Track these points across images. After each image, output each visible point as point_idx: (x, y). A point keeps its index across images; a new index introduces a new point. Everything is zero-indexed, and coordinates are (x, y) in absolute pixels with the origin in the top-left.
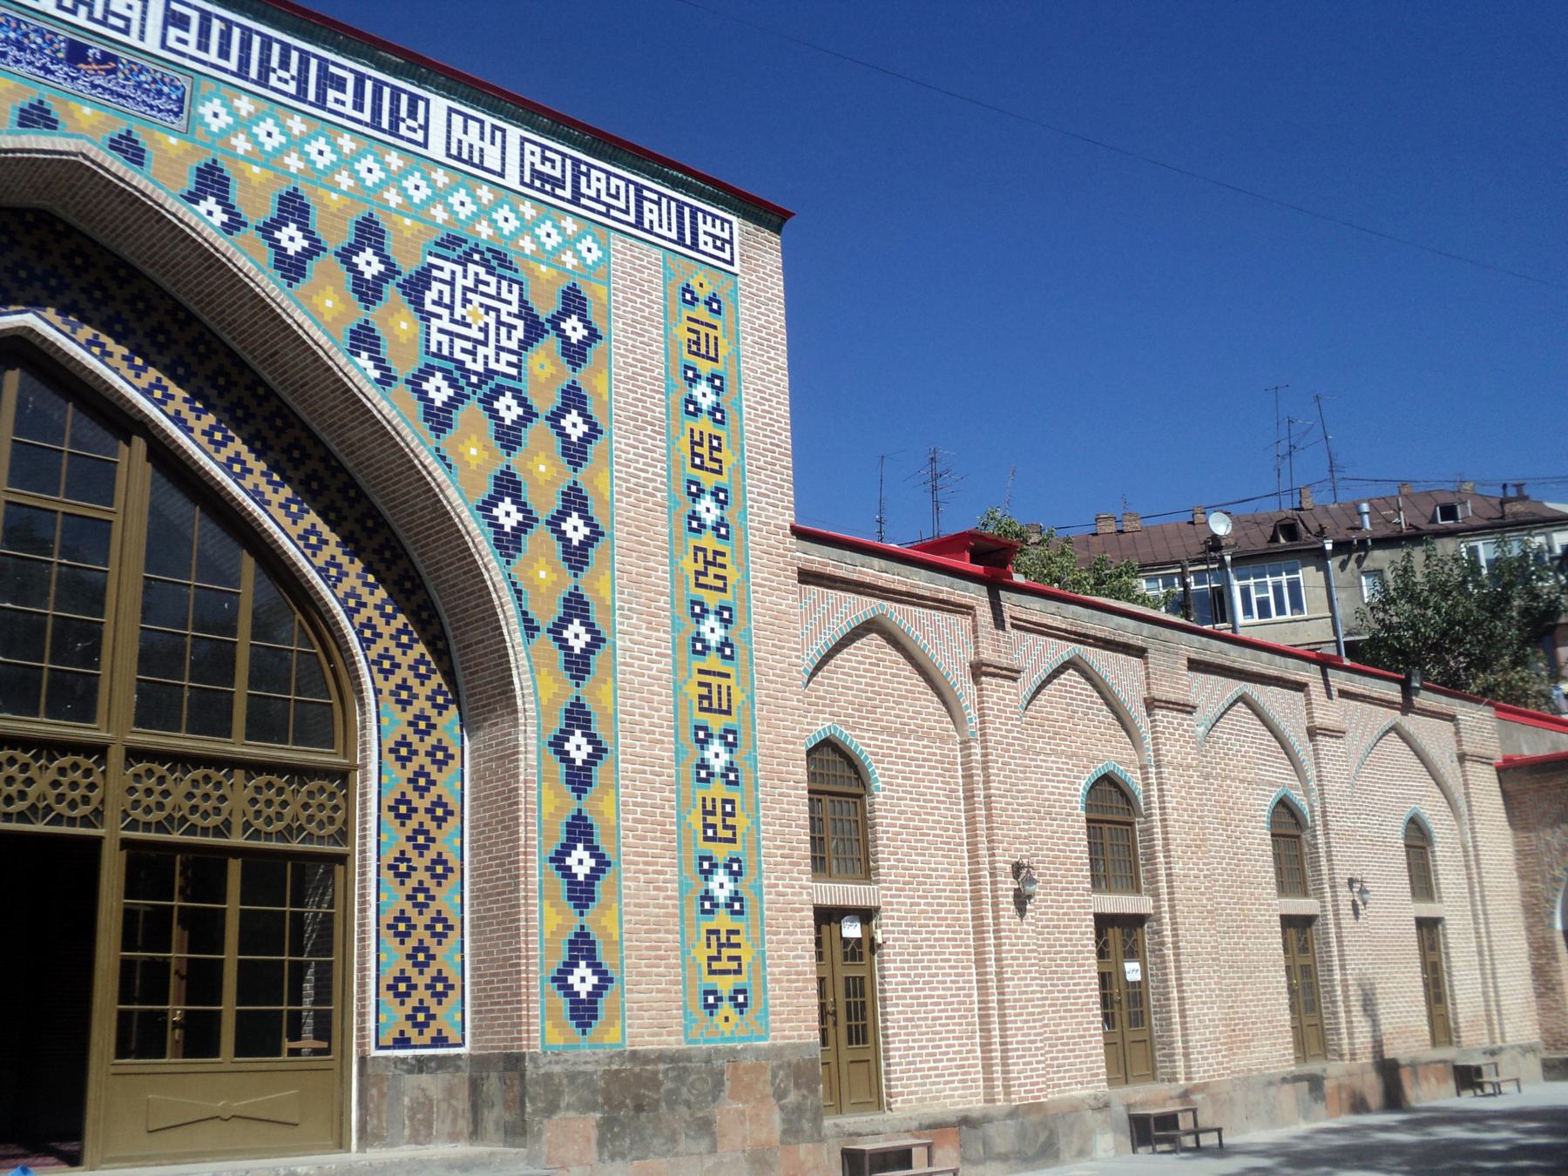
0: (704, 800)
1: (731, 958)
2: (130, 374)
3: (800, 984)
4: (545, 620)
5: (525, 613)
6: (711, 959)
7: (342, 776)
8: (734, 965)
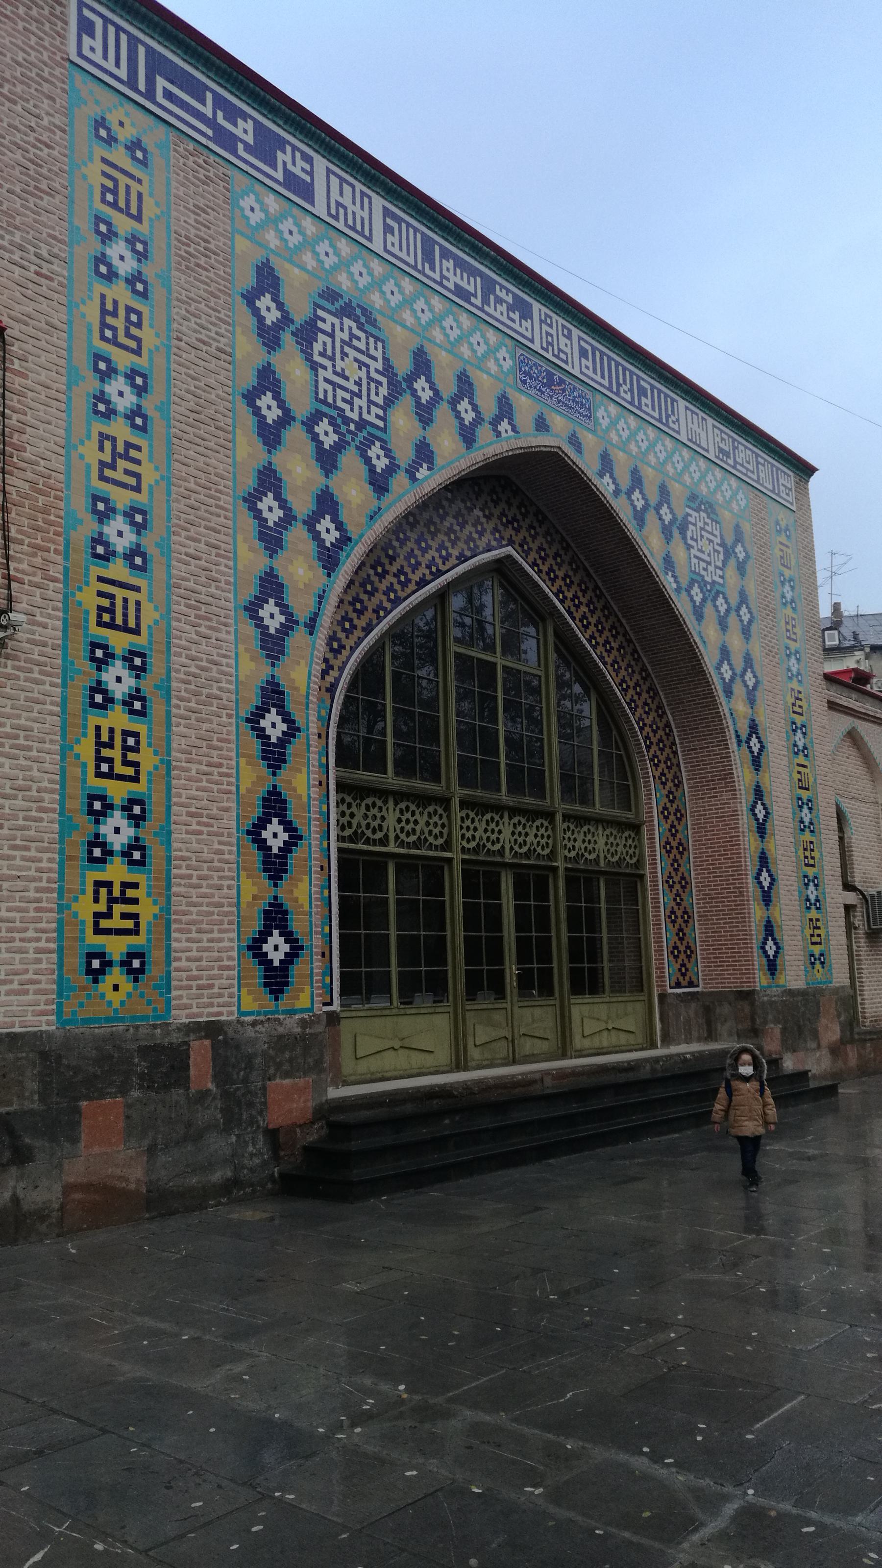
2: (549, 583)
7: (636, 828)
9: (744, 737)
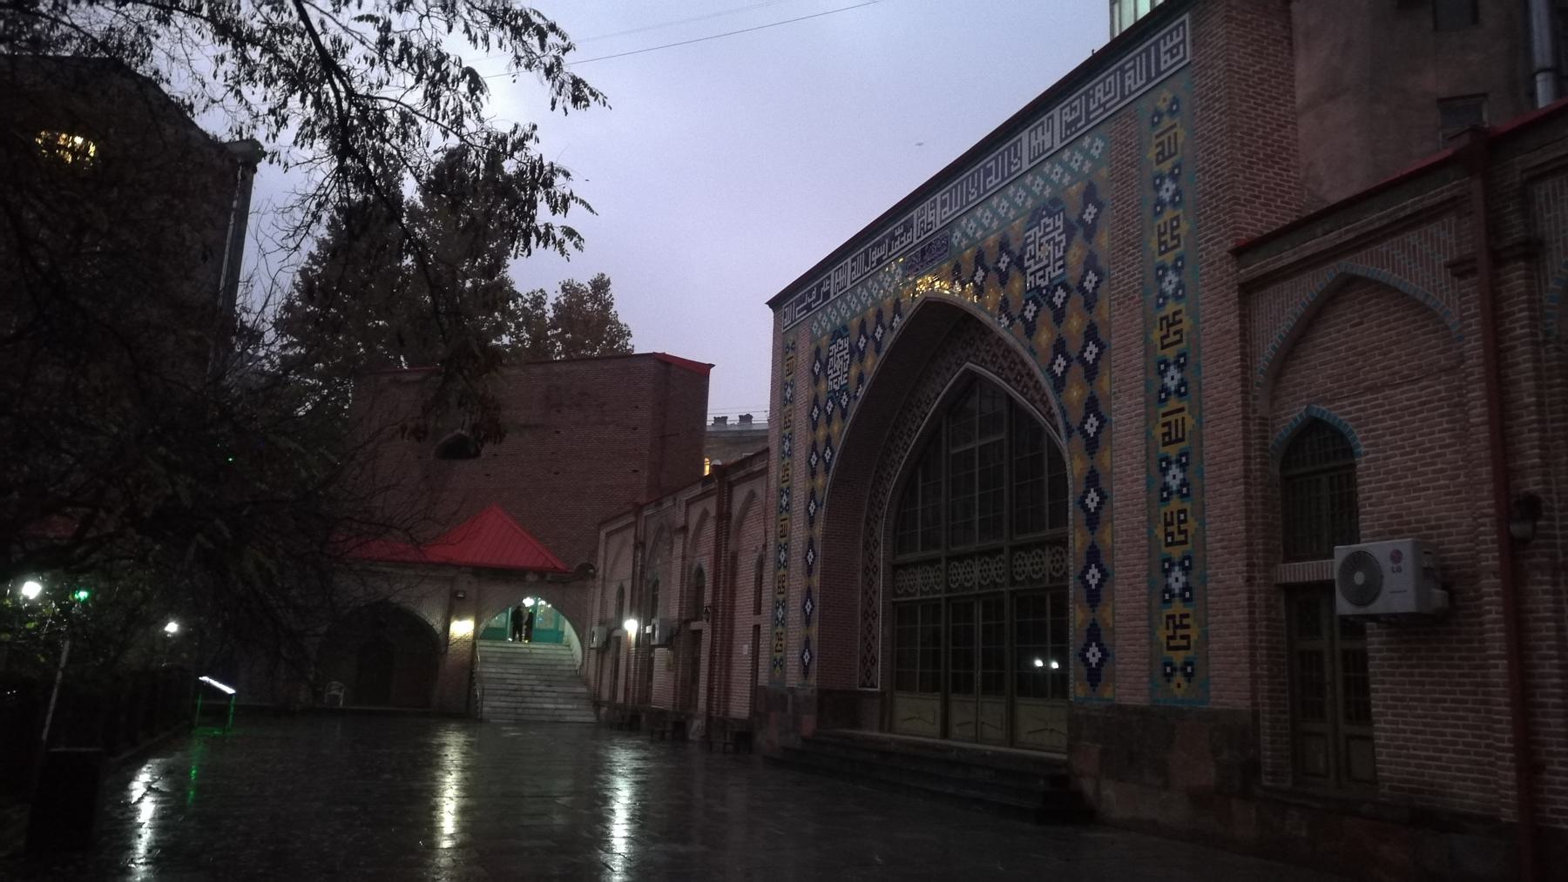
0: (1166, 514)
1: (1183, 637)
3: (1235, 659)
4: (1075, 424)
5: (1067, 423)
6: (1170, 638)
8: (1184, 643)
9: (1075, 424)
